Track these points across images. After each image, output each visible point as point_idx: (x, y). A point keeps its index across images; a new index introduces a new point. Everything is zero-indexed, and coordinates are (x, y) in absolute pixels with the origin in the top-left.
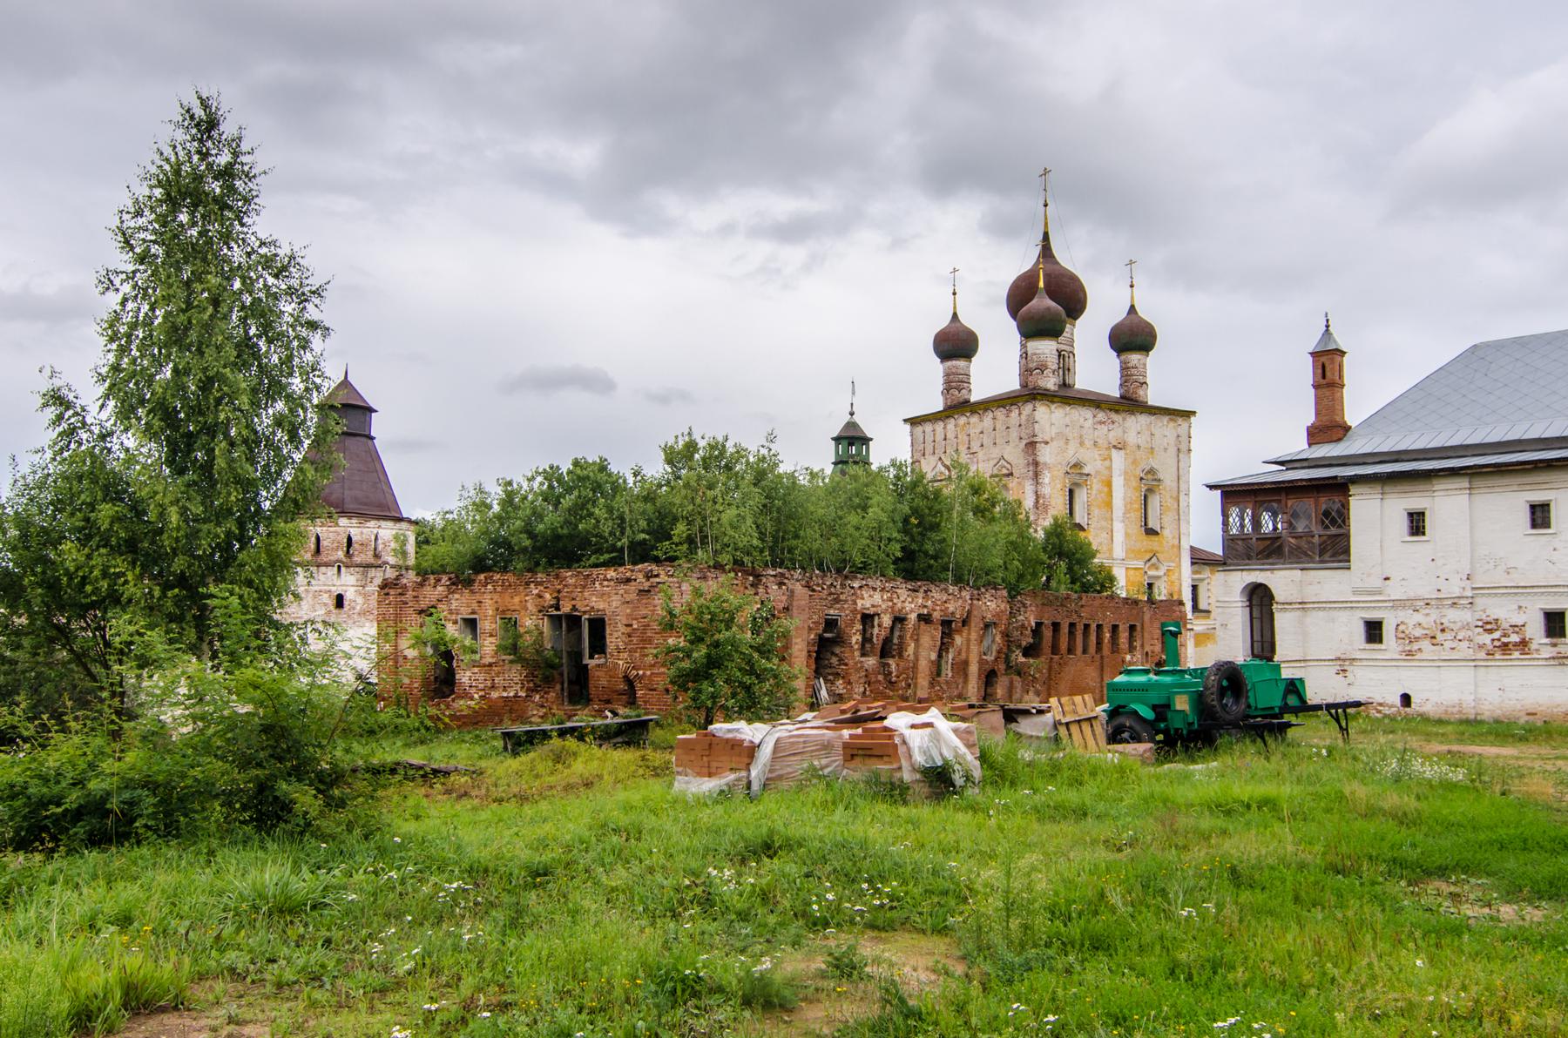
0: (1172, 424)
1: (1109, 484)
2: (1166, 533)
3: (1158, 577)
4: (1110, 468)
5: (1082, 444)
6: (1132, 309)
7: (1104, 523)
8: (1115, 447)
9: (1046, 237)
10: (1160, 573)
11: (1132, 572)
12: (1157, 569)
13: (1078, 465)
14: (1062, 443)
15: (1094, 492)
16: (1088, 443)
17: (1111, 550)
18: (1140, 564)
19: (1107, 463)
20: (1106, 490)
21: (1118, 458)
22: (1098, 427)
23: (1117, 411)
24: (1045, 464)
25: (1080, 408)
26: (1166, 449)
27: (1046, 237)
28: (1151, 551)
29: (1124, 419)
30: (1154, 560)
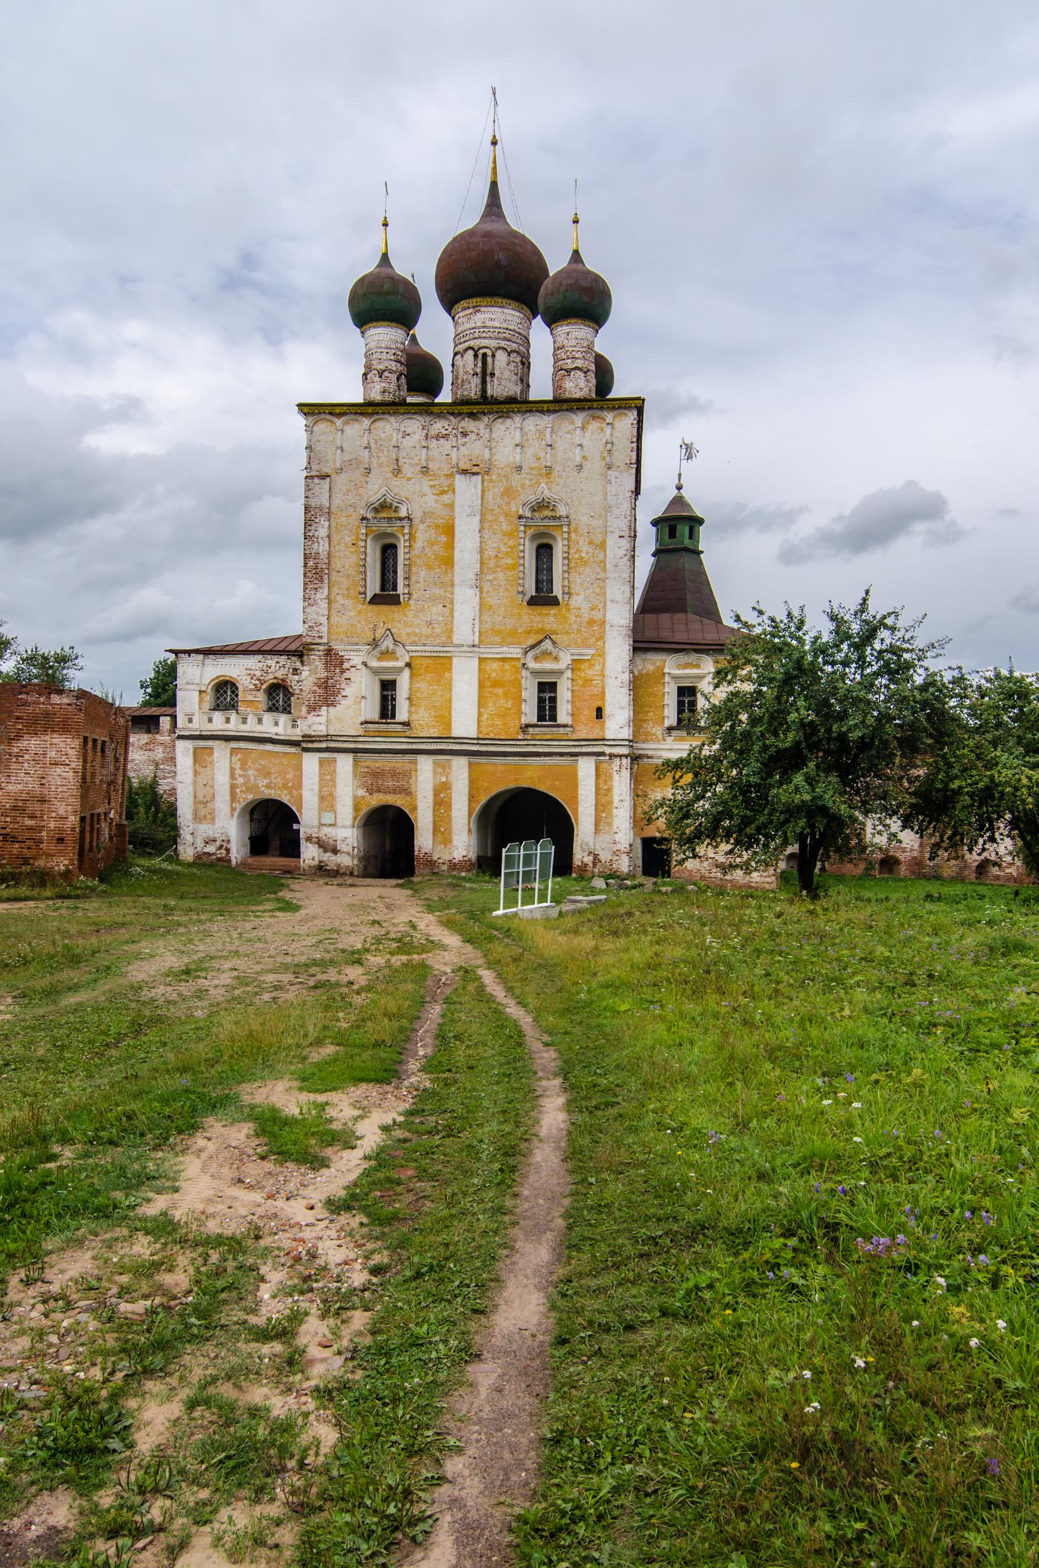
0: (594, 425)
1: (449, 530)
2: (577, 601)
3: (560, 673)
4: (451, 506)
5: (397, 471)
6: (576, 256)
7: (438, 592)
8: (464, 472)
9: (494, 185)
10: (561, 665)
11: (495, 665)
12: (556, 659)
13: (383, 506)
14: (357, 476)
15: (419, 544)
16: (407, 470)
17: (449, 632)
18: (515, 652)
19: (446, 498)
20: (443, 539)
21: (467, 491)
22: (434, 444)
23: (473, 416)
24: (321, 509)
25: (392, 419)
26: (580, 467)
27: (494, 185)
28: (542, 630)
29: (489, 427)
30: (547, 645)
